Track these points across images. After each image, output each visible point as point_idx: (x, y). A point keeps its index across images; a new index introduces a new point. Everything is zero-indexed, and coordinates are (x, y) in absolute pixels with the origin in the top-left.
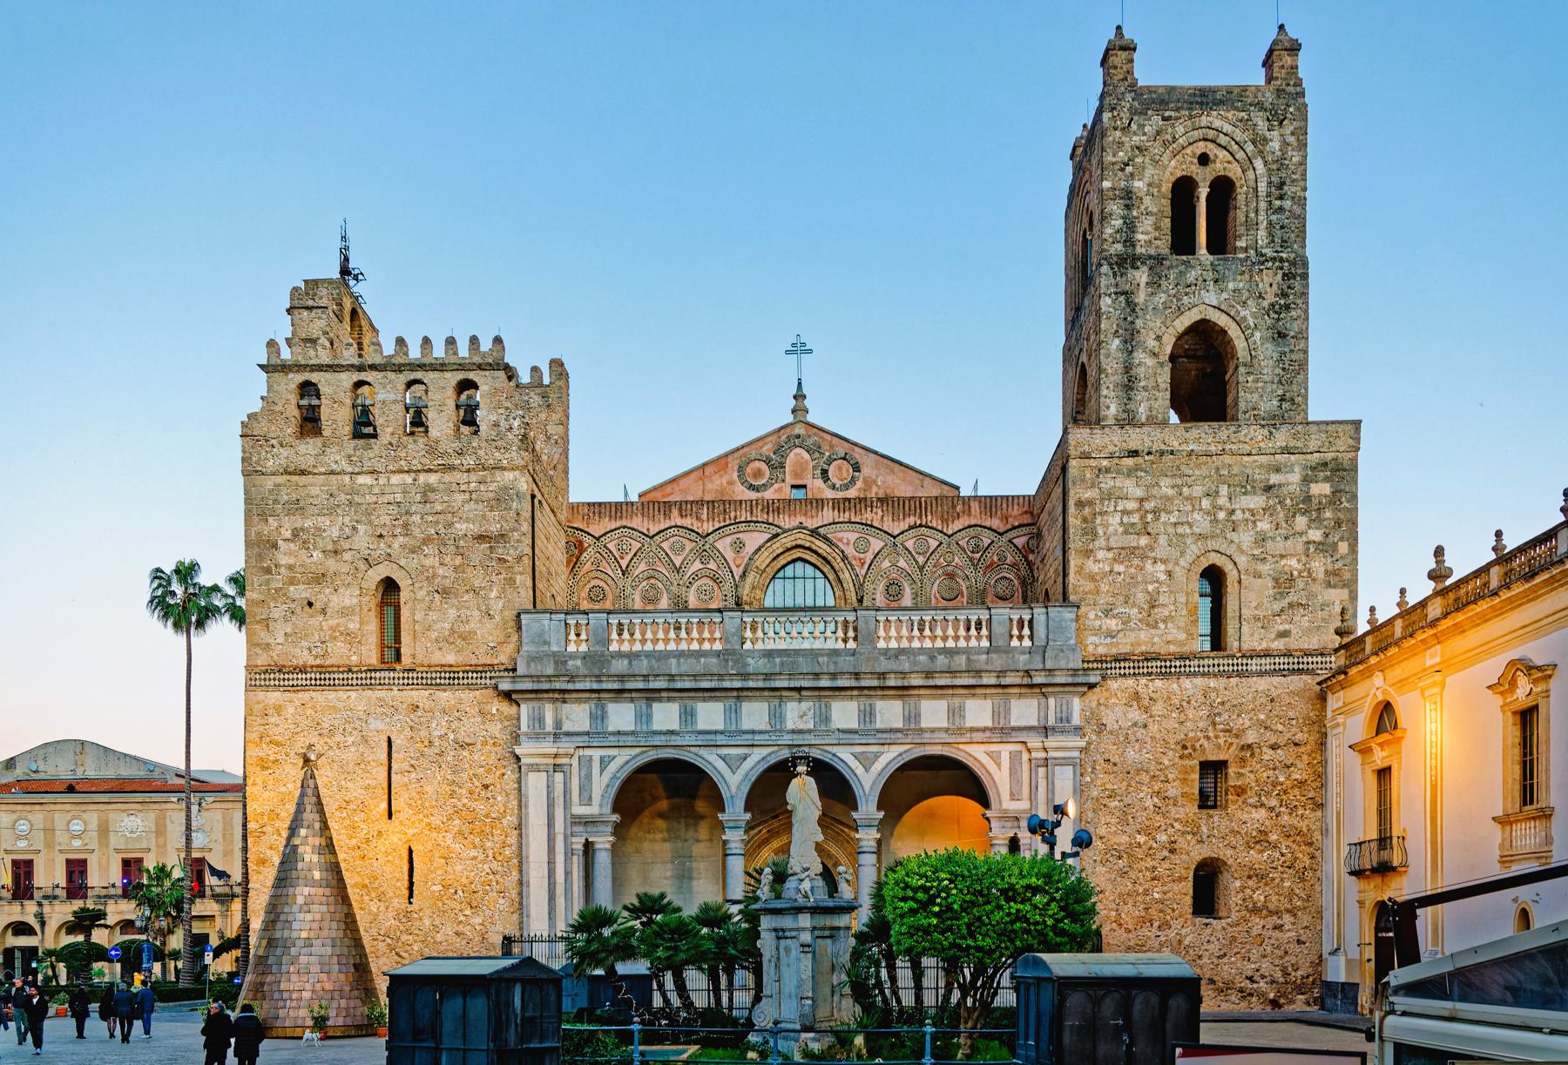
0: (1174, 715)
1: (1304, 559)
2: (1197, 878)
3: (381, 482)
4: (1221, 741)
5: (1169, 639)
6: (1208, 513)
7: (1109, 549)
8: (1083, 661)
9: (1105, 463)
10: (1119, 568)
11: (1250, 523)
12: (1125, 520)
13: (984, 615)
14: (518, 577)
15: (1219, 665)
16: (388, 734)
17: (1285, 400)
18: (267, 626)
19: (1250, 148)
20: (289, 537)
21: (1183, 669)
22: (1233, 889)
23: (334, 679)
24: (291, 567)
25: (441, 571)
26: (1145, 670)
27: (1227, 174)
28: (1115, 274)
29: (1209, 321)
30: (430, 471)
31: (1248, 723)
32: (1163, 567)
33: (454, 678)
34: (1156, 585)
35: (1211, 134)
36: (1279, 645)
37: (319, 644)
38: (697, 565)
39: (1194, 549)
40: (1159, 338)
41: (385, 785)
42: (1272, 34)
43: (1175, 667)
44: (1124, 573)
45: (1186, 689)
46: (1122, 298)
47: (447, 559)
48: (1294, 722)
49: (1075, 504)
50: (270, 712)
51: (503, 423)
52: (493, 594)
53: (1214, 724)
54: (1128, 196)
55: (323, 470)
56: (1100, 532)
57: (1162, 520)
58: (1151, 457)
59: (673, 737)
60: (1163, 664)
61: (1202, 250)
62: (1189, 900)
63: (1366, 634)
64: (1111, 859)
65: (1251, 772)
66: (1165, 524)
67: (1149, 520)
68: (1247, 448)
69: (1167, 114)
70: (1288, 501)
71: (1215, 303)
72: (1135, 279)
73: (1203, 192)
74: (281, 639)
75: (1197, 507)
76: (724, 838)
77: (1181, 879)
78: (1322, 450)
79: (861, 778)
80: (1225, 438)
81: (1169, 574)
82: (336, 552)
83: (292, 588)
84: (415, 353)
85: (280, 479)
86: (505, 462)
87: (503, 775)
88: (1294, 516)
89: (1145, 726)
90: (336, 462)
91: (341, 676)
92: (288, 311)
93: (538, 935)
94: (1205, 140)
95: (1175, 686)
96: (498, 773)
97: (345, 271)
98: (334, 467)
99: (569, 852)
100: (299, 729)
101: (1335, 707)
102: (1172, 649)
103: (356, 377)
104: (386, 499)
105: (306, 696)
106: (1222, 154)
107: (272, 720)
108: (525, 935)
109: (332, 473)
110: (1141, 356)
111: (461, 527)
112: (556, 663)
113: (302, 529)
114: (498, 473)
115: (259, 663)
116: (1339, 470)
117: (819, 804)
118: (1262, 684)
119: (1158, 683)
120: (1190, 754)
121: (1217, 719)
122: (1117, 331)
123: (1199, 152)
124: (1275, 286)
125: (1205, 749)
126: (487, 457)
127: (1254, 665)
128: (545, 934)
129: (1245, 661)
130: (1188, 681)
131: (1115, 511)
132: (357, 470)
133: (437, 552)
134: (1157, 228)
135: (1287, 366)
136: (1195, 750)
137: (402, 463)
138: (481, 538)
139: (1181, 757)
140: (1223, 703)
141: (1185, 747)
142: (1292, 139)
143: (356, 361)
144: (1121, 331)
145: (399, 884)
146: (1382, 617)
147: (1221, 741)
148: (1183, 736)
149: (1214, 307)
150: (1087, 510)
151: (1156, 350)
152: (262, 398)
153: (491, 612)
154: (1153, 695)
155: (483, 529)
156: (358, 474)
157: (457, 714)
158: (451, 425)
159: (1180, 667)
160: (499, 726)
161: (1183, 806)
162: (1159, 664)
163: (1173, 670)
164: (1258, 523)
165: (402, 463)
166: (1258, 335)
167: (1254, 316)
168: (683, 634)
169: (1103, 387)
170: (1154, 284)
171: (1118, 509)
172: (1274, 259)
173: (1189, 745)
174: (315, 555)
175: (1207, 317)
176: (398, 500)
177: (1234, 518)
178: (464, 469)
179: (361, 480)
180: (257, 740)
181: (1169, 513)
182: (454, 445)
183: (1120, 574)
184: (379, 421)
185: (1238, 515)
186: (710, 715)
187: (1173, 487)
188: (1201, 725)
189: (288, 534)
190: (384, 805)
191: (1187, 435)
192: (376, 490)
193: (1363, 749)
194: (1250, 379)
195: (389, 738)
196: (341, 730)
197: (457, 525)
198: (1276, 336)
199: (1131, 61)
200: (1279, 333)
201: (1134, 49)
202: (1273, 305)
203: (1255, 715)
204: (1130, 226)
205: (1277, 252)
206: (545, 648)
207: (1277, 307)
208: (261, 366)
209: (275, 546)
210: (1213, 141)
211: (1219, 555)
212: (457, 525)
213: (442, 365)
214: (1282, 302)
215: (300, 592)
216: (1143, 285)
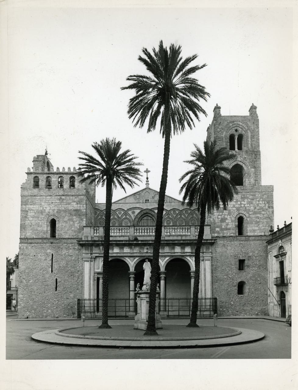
2: (238, 286)
6: (240, 205)
11: (249, 207)
16: (52, 253)
22: (246, 289)
27: (242, 133)
32: (229, 217)
35: (238, 125)
38: (124, 217)
39: (237, 213)
41: (51, 264)
42: (251, 105)
59: (118, 254)
61: (236, 149)
62: (237, 291)
63: (276, 231)
71: (240, 160)
76: (130, 277)
77: (235, 286)
80: (243, 189)
84: (61, 171)
85: (29, 197)
87: (79, 262)
90: (42, 193)
92: (33, 161)
93: (86, 299)
96: (77, 262)
97: (46, 154)
98: (42, 194)
99: (94, 280)
103: (48, 175)
105: (33, 245)
106: (240, 129)
108: (83, 299)
109: (41, 196)
112: (92, 237)
117: (151, 268)
123: (235, 129)
125: (240, 257)
128: (88, 299)
132: (47, 195)
136: (237, 257)
143: (48, 172)
145: (54, 287)
146: (280, 228)
152: (26, 180)
158: (69, 186)
164: (251, 207)
168: (121, 231)
173: (236, 256)
179: (48, 197)
184: (52, 185)
186: (126, 250)
190: (51, 269)
193: (276, 257)
195: (52, 254)
199: (220, 111)
201: (220, 108)
208: (26, 173)
213: (67, 173)
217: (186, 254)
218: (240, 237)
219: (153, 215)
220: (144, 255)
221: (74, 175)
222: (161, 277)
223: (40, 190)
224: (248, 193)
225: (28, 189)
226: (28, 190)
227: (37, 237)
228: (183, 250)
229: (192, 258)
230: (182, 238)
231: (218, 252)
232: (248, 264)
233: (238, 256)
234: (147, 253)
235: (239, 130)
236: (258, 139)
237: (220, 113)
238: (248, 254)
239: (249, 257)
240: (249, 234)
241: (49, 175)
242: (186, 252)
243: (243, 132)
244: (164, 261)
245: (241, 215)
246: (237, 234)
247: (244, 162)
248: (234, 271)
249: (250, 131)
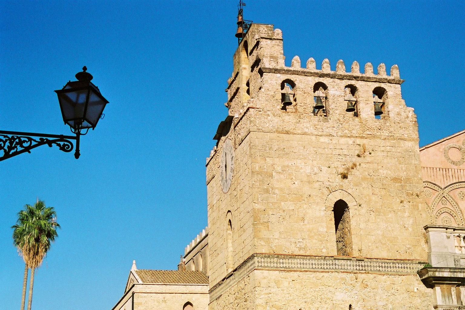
3: (334, 142)
14: (420, 205)
18: (268, 227)
20: (280, 171)
23: (312, 264)
24: (281, 190)
25: (374, 198)
30: (362, 137)
33: (388, 267)
37: (301, 240)
47: (377, 191)
50: (272, 284)
51: (403, 113)
52: (407, 214)
55: (299, 132)
74: (277, 235)
82: (309, 182)
83: (283, 203)
86: (406, 136)
91: (316, 262)
98: (306, 130)
100: (292, 297)
104: (337, 152)
105: (296, 274)
107: (273, 290)
111: (383, 172)
113: (288, 166)
114: (402, 142)
115: (264, 252)
126: (395, 132)
132: (320, 133)
133: (370, 187)
137: (347, 131)
138: (396, 180)
153: (406, 226)
155: (396, 174)
156: (321, 136)
157: (393, 291)
160: (419, 301)
165: (347, 131)
174: (296, 183)
176: (345, 153)
178: (383, 137)
179: (322, 139)
180: (264, 304)
182: (376, 124)
189: (279, 169)
192: (332, 147)
195: (350, 306)
196: (319, 300)
197: (381, 171)
206: (445, 251)
209: (271, 176)
212: (381, 171)
215: (289, 205)
221: (382, 85)
223: (300, 117)
225: (269, 113)
226: (268, 115)
227: (302, 253)
241: (321, 80)
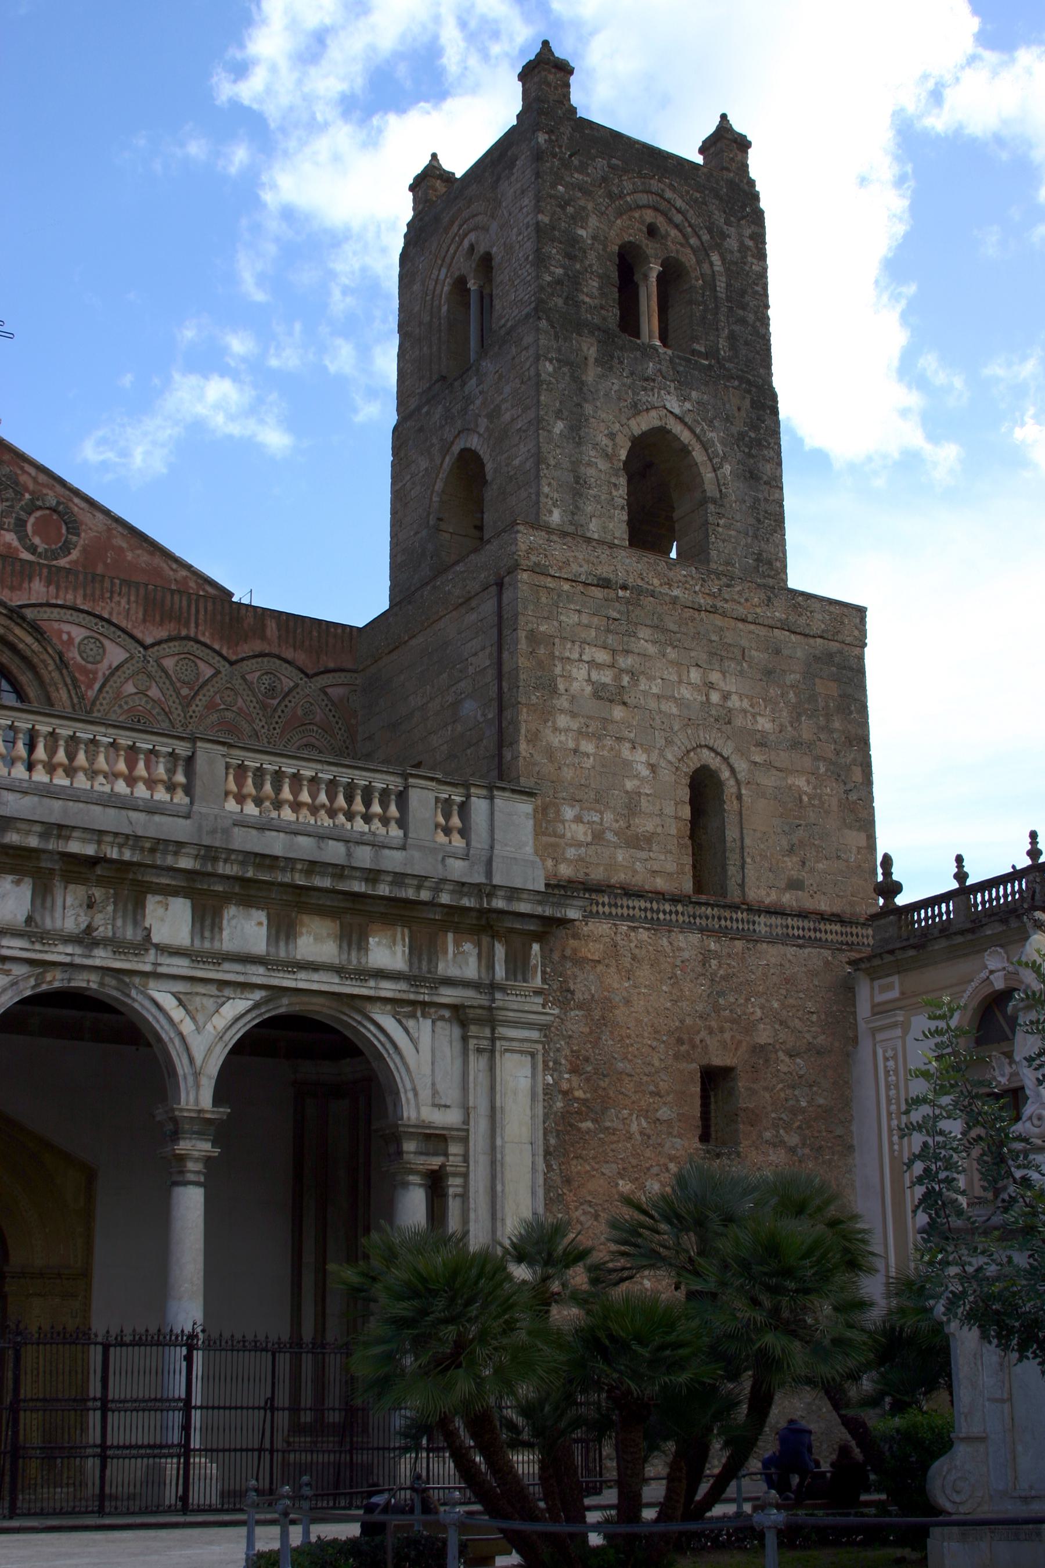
0: (664, 988)
1: (813, 779)
4: (727, 1036)
5: (655, 868)
7: (573, 715)
8: (547, 885)
9: (566, 587)
10: (588, 747)
12: (594, 676)
13: (394, 783)
15: (719, 919)
17: (761, 561)
19: (706, 237)
21: (674, 917)
26: (625, 911)
28: (556, 334)
29: (669, 432)
31: (759, 1013)
32: (644, 758)
34: (636, 782)
35: (664, 205)
36: (788, 899)
39: (682, 741)
40: (612, 436)
43: (664, 912)
44: (595, 755)
45: (680, 949)
46: (565, 369)
48: (814, 1018)
49: (526, 637)
53: (717, 1009)
54: (573, 241)
56: (561, 687)
57: (642, 688)
58: (621, 593)
60: (648, 905)
64: (582, 1218)
65: (766, 1089)
66: (645, 693)
67: (625, 683)
68: (741, 611)
69: (614, 161)
70: (791, 695)
71: (677, 411)
72: (581, 350)
73: (655, 269)
75: (684, 678)
78: (825, 635)
79: (190, 1040)
81: (653, 767)
88: (798, 719)
89: (628, 1002)
94: (656, 209)
95: (665, 942)
101: (880, 998)
102: (660, 883)
106: (673, 232)
110: (592, 453)
116: (844, 668)
118: (772, 954)
119: (643, 935)
120: (689, 1054)
121: (721, 1001)
122: (560, 411)
124: (743, 414)
127: (763, 924)
129: (751, 917)
130: (681, 937)
131: (580, 660)
134: (603, 295)
135: (761, 517)
136: (694, 1047)
139: (676, 1057)
140: (725, 978)
141: (680, 1041)
142: (751, 243)
144: (566, 413)
147: (727, 1036)
148: (677, 1024)
149: (676, 416)
150: (542, 651)
151: (610, 450)
154: (637, 951)
159: (671, 912)
161: (680, 1136)
162: (643, 904)
163: (661, 916)
164: (759, 718)
166: (727, 468)
167: (724, 444)
169: (544, 482)
170: (606, 361)
171: (585, 658)
172: (739, 378)
173: (685, 1037)
175: (668, 427)
177: (730, 704)
181: (651, 678)
183: (588, 755)
185: (734, 702)
187: (654, 642)
188: (700, 1007)
191: (671, 574)
194: (722, 522)
198: (748, 475)
200: (751, 472)
202: (742, 435)
203: (767, 1001)
204: (574, 281)
205: (742, 370)
207: (747, 439)
210: (664, 214)
211: (713, 755)
214: (752, 435)
216: (591, 360)
217: (372, 983)
218: (709, 911)
219: (24, 659)
220: (60, 953)
222: (182, 1159)
224: (740, 625)
228: (354, 954)
229: (411, 1024)
230: (349, 855)
231: (578, 996)
232: (751, 1106)
233: (698, 1042)
234: (87, 939)
235: (668, 234)
236: (764, 321)
237: (567, 96)
238: (750, 1028)
239: (759, 1050)
240: (758, 892)
242: (381, 974)
243: (688, 251)
244: (209, 1027)
245: (707, 757)
246: (687, 886)
247: (698, 431)
248: (673, 1147)
249: (723, 259)
